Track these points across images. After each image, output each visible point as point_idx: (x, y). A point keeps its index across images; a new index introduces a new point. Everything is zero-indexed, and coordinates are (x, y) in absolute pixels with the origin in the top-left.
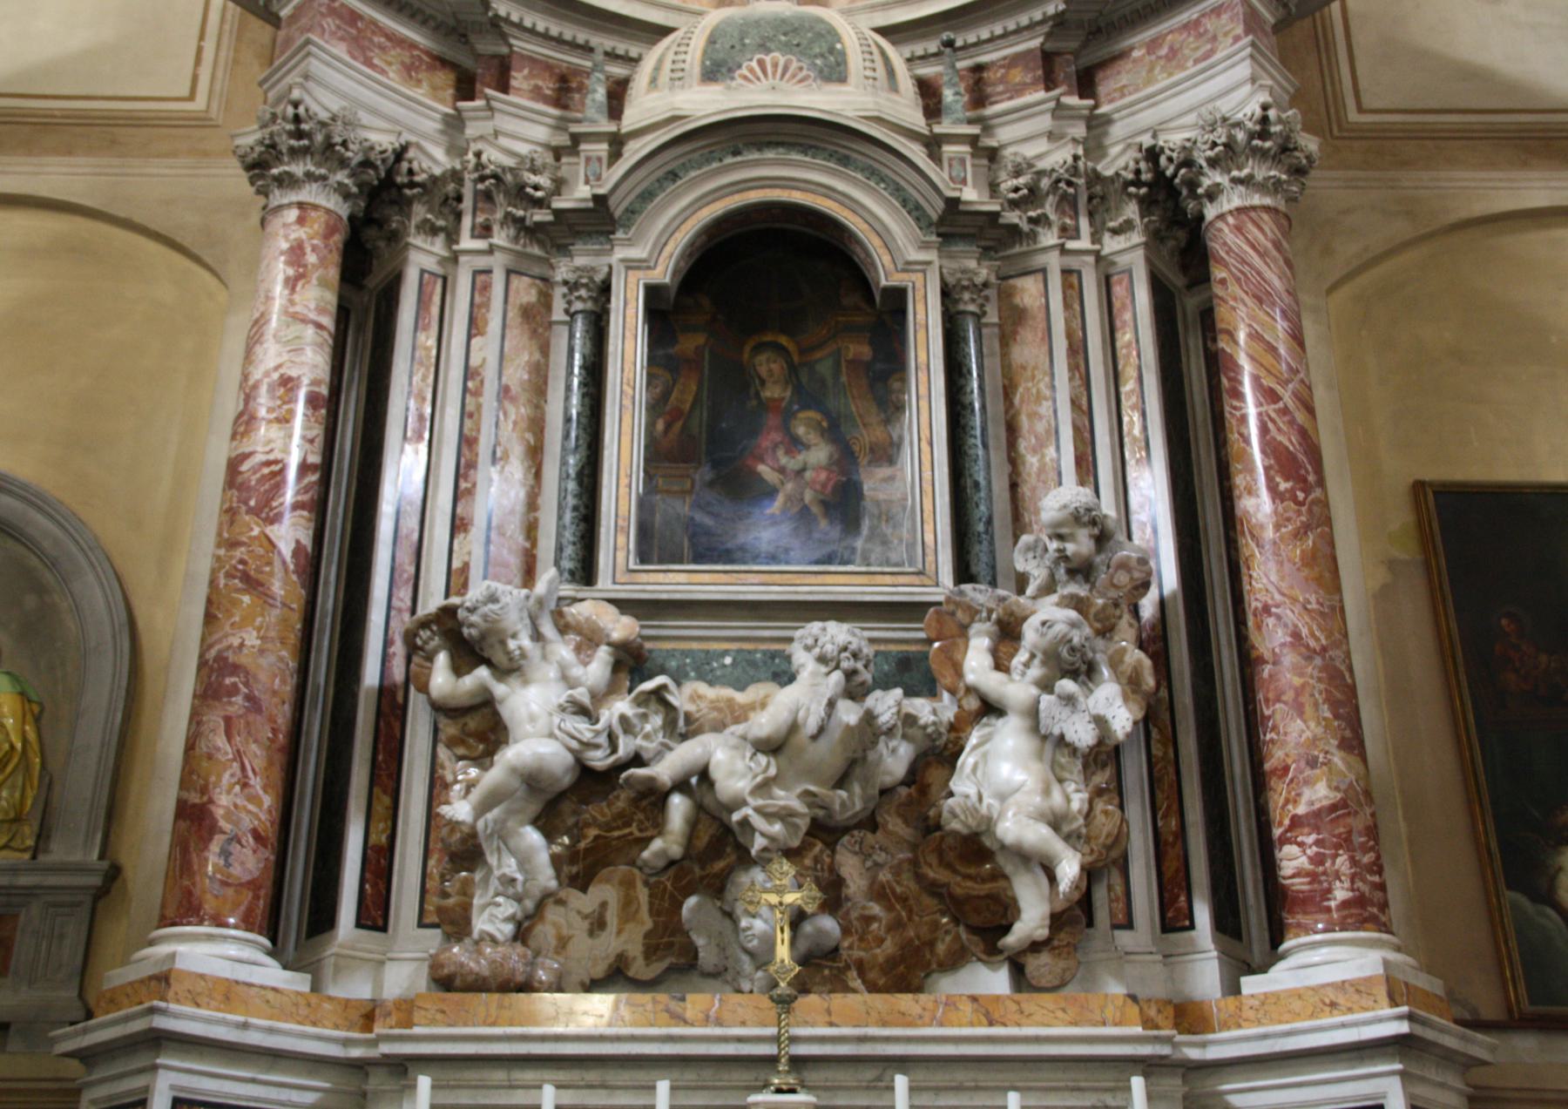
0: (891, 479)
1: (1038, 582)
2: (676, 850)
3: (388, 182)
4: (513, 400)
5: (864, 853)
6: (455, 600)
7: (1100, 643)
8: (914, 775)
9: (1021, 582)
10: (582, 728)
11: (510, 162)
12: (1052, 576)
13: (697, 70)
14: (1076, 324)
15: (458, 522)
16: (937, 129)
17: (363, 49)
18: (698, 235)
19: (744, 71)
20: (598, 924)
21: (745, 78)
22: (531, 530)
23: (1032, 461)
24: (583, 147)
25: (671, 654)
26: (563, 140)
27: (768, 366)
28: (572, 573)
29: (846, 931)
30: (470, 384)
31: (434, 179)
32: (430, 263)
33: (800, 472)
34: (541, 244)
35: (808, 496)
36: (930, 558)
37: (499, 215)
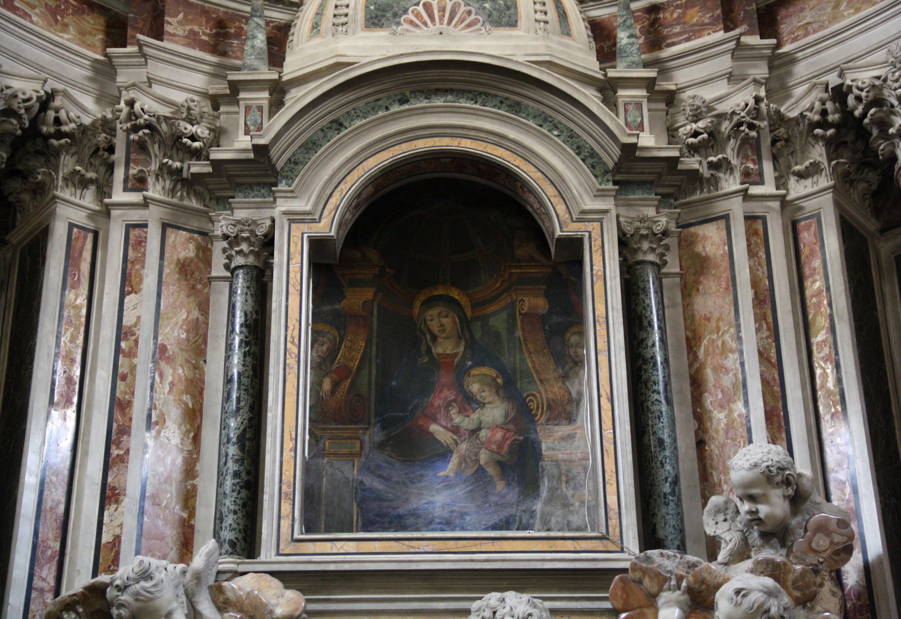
0: (571, 437)
1: (730, 546)
3: (33, 132)
4: (170, 360)
6: (103, 578)
9: (712, 547)
11: (165, 111)
12: (745, 540)
13: (361, 16)
14: (762, 272)
15: (108, 492)
16: (611, 73)
18: (365, 186)
19: (410, 16)
21: (411, 22)
22: (188, 498)
23: (719, 417)
24: (242, 95)
26: (221, 88)
27: (439, 320)
28: (232, 544)
30: (123, 344)
31: (83, 129)
32: (80, 217)
33: (475, 432)
34: (199, 196)
35: (484, 457)
36: (614, 522)
37: (154, 167)
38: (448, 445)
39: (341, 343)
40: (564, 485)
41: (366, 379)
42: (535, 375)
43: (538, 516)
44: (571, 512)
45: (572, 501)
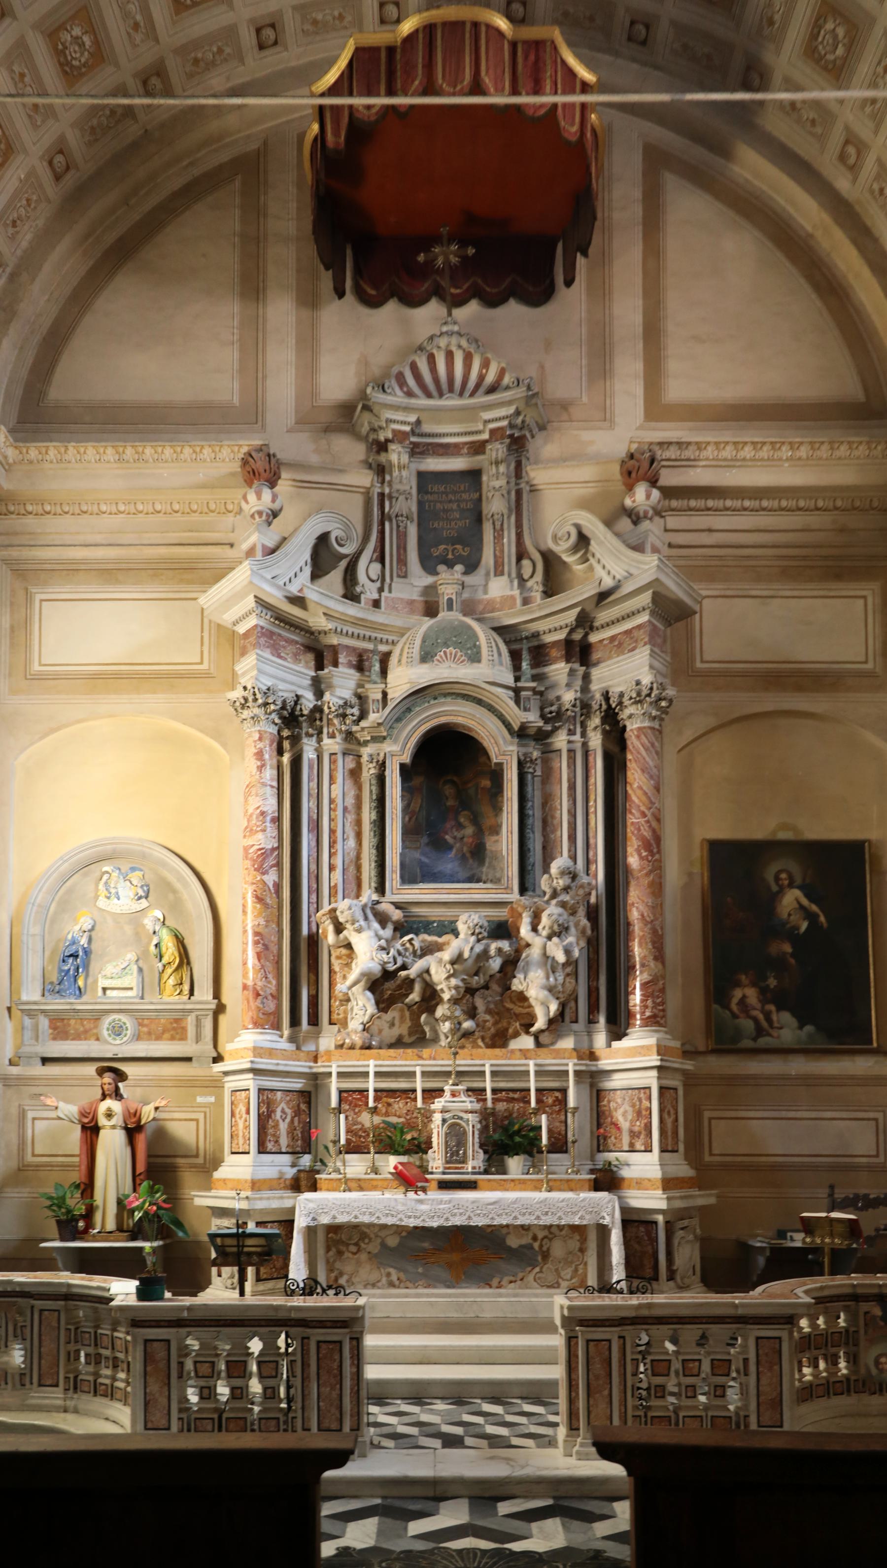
0: (497, 841)
2: (417, 999)
5: (484, 998)
7: (572, 918)
8: (502, 969)
10: (385, 957)
17: (277, 650)
20: (392, 1025)
22: (359, 868)
25: (414, 922)
29: (478, 1025)
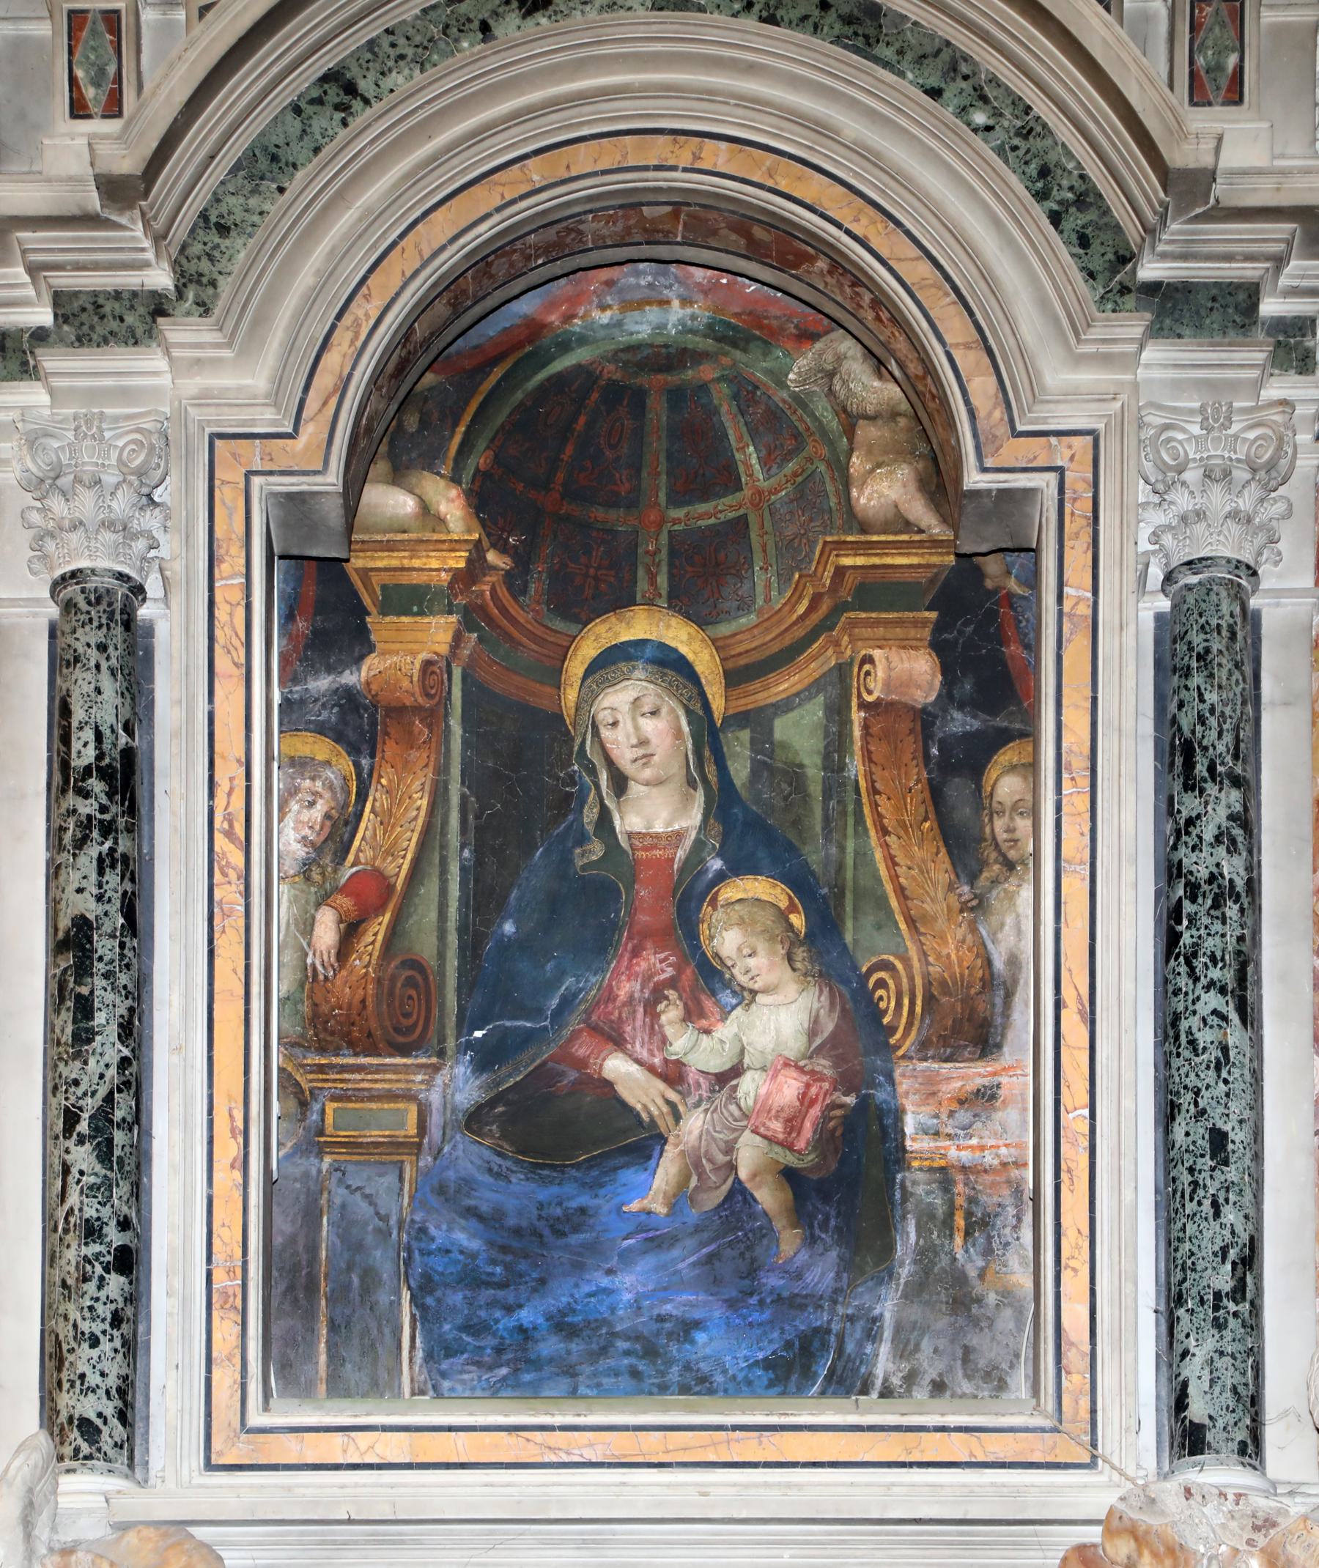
33: (727, 1078)
35: (750, 1153)
38: (653, 1121)
39: (362, 796)
40: (959, 1240)
41: (433, 915)
42: (894, 903)
43: (887, 1334)
44: (975, 1322)
45: (978, 1289)
